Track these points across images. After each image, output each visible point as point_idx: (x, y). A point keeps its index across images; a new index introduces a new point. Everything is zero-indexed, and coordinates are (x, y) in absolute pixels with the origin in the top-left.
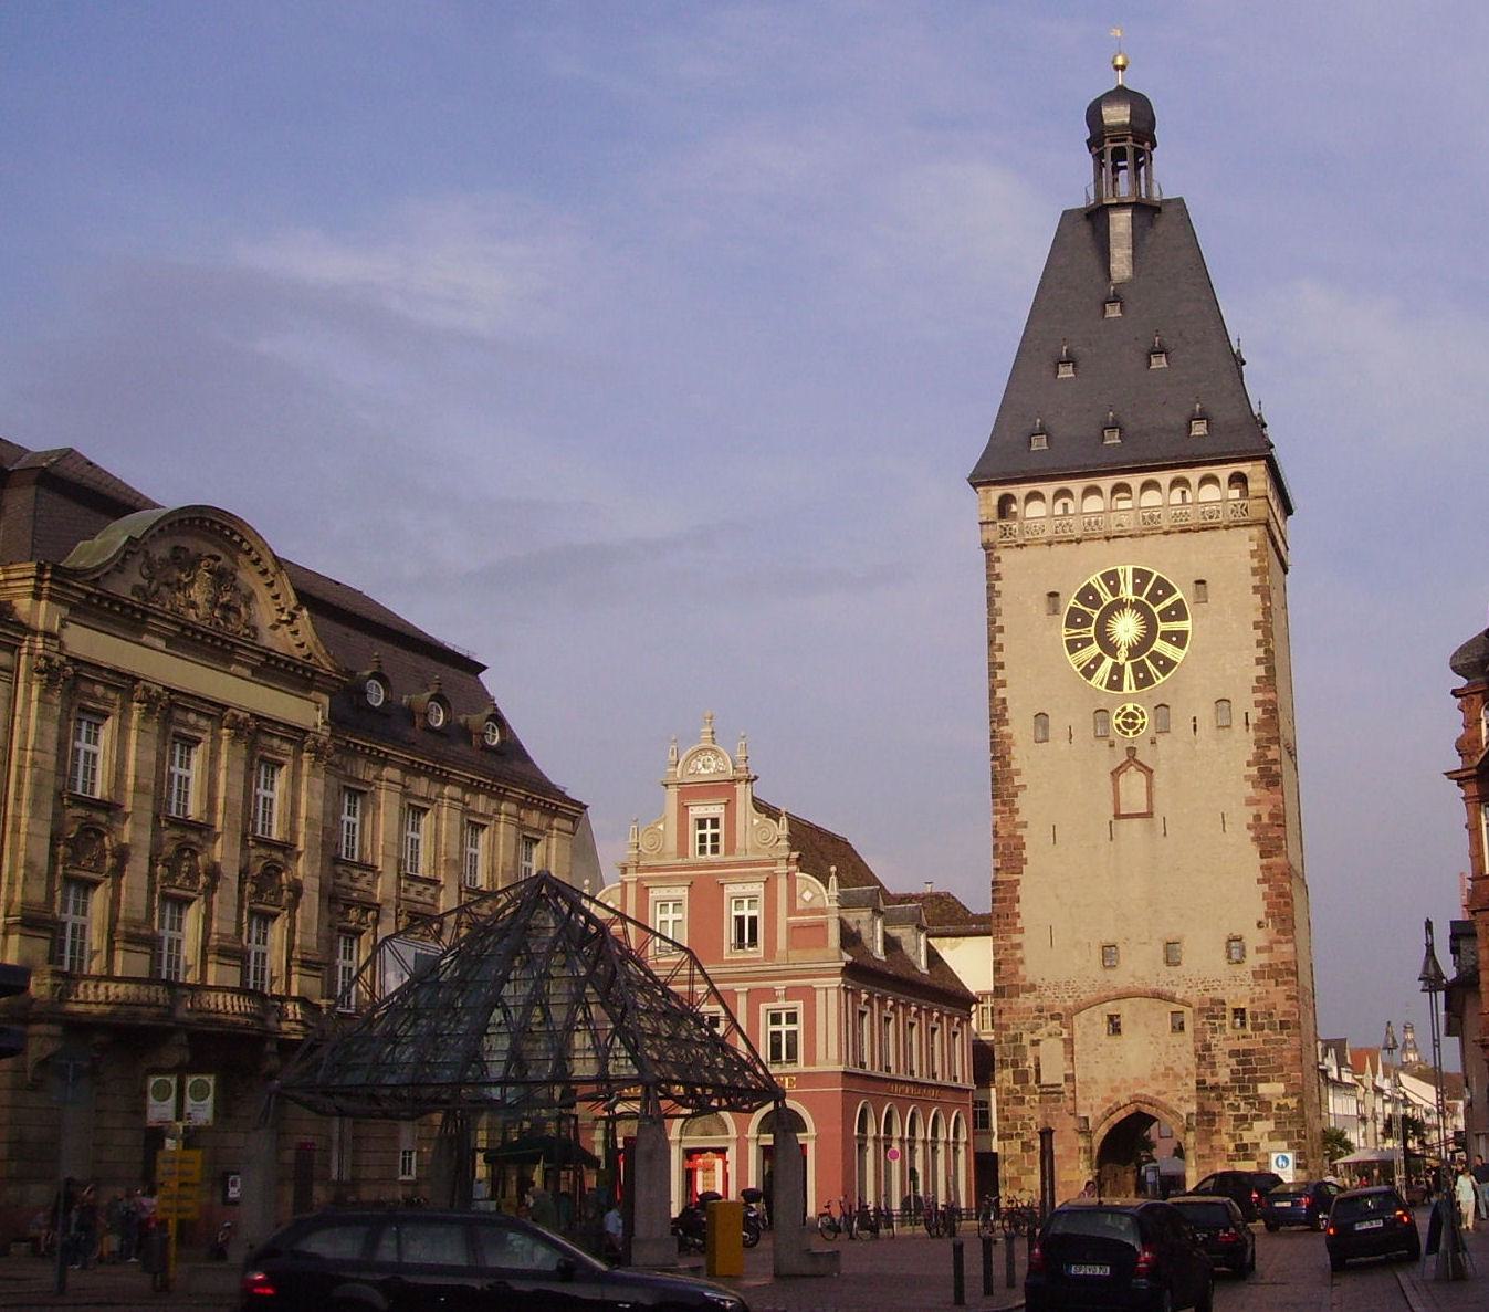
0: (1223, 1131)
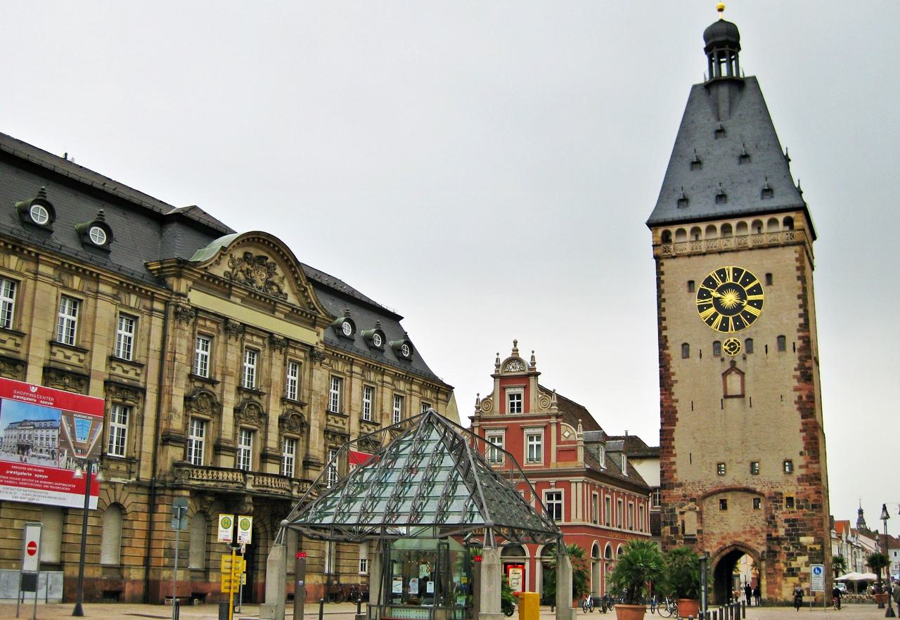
0: (781, 560)
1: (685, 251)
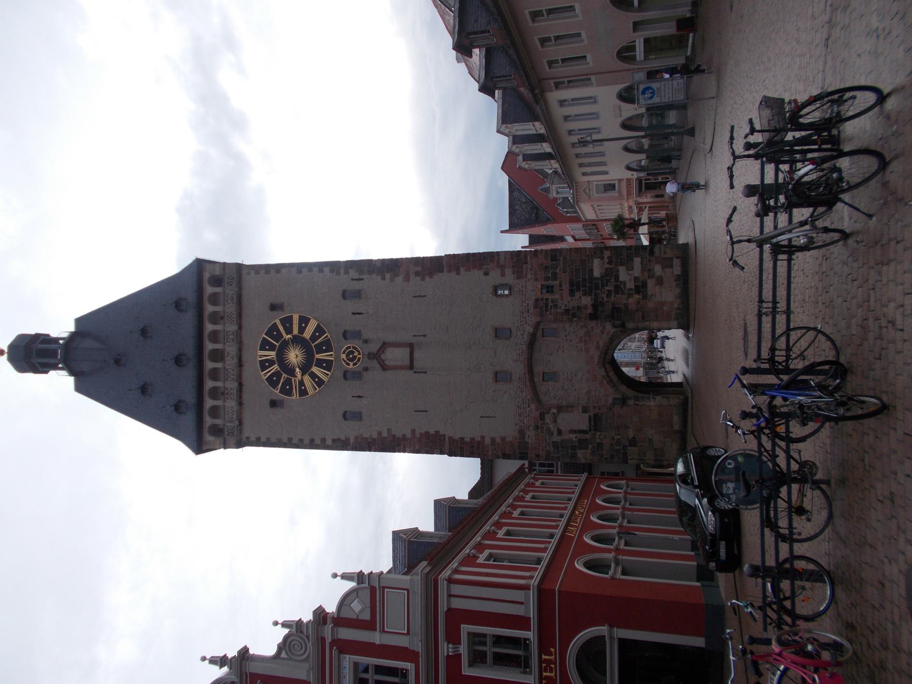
0: (625, 302)
1: (235, 409)
